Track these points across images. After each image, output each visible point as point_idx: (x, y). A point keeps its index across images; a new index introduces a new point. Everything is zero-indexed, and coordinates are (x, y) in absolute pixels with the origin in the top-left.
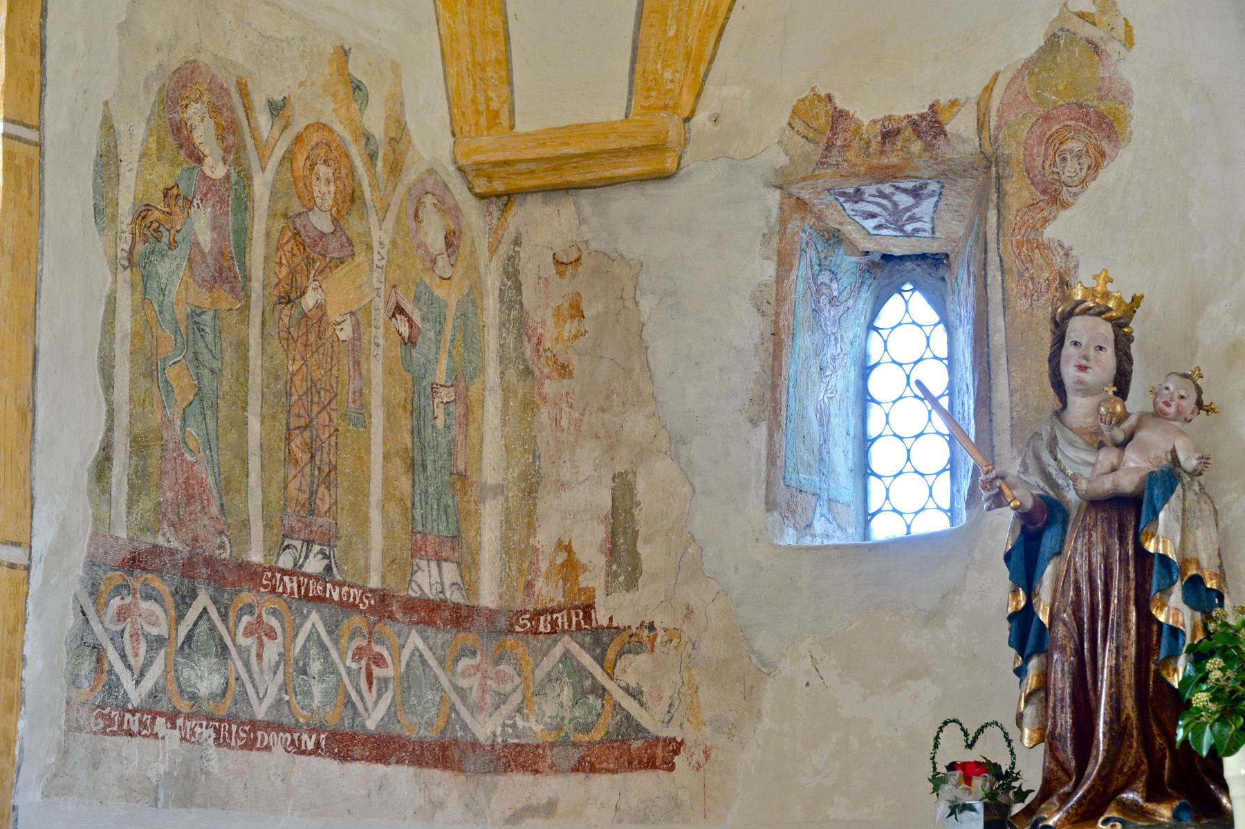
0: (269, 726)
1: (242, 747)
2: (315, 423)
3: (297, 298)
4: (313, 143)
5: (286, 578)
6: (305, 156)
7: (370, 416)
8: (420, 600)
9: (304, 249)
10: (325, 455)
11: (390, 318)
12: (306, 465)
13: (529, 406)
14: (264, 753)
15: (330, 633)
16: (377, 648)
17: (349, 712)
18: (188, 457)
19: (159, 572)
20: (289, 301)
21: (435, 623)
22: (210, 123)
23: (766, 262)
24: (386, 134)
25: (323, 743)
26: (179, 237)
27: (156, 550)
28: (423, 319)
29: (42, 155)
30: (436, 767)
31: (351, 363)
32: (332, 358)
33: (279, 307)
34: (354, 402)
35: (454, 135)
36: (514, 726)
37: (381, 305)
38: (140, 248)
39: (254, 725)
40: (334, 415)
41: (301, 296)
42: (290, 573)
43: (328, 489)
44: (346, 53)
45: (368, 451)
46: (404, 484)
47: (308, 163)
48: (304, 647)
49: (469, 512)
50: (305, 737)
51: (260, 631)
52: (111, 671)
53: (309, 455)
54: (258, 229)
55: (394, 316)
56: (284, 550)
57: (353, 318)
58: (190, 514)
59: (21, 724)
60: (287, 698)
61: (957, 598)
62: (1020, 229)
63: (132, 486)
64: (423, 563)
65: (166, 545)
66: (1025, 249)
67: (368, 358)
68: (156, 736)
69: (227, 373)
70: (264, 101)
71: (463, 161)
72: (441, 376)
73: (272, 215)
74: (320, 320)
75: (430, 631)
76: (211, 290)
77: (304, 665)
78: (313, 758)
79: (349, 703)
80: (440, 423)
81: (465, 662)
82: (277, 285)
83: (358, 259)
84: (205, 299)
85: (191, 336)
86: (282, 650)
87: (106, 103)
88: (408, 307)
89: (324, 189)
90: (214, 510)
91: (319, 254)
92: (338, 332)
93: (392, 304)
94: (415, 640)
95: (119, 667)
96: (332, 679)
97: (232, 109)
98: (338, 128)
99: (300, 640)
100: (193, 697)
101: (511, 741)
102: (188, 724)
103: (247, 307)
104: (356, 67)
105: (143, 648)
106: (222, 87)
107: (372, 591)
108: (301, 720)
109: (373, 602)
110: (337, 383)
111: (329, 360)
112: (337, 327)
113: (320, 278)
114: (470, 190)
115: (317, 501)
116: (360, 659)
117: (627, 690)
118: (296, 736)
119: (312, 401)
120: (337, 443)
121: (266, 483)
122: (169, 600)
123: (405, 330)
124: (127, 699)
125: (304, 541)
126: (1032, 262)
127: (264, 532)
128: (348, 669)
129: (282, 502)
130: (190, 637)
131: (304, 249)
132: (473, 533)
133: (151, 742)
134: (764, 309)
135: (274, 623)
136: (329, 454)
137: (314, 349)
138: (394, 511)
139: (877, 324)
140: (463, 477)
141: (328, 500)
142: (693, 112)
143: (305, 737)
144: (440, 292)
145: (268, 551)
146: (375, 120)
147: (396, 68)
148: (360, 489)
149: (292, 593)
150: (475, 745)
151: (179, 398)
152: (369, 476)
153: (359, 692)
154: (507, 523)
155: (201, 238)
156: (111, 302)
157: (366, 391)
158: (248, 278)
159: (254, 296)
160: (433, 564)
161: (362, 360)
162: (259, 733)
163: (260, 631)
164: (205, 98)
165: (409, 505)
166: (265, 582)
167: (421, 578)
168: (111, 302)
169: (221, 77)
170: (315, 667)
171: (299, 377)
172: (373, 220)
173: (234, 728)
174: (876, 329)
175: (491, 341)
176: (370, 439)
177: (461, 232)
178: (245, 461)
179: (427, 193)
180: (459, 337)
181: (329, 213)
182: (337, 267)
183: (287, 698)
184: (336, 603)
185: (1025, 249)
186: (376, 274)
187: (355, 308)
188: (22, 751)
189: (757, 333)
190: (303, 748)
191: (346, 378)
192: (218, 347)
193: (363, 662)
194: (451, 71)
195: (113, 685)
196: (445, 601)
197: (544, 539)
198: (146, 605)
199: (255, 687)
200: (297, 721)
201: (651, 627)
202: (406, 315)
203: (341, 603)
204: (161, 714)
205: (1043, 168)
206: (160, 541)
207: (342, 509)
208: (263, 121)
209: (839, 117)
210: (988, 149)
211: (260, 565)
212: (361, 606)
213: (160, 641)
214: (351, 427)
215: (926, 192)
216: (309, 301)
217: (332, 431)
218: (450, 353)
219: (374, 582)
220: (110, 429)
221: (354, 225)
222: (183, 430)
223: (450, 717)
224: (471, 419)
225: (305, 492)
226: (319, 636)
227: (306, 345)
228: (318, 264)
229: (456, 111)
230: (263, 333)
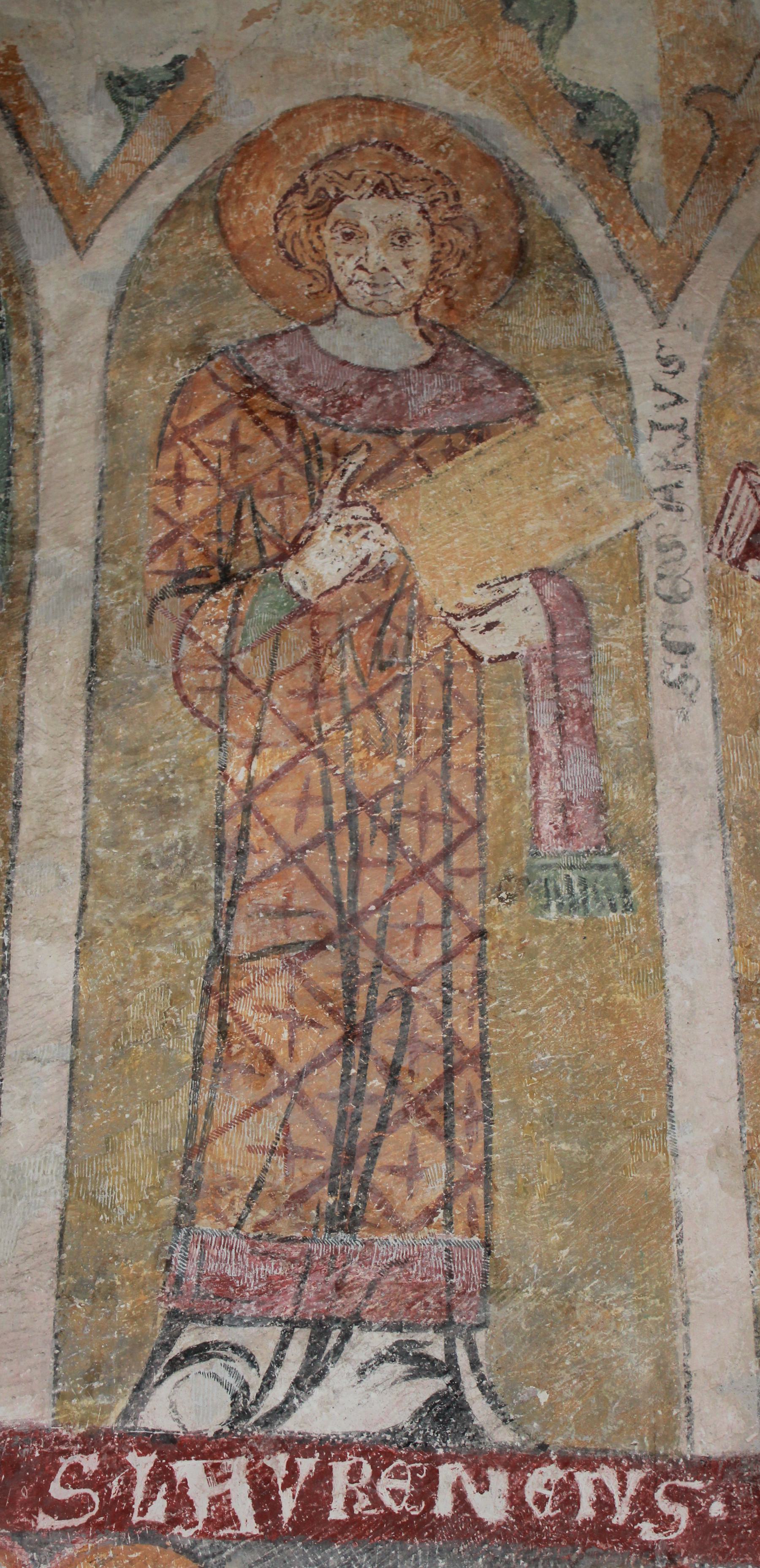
2: (370, 925)
3: (264, 564)
4: (321, 151)
6: (283, 184)
7: (654, 868)
9: (292, 425)
10: (423, 1018)
11: (739, 563)
12: (316, 1064)
20: (227, 578)
24: (666, 79)
31: (544, 721)
32: (447, 717)
33: (176, 605)
34: (568, 834)
41: (283, 557)
47: (299, 203)
53: (337, 1031)
56: (174, 1365)
57: (549, 590)
70: (89, 80)
74: (385, 612)
82: (168, 542)
83: (551, 420)
89: (376, 256)
91: (365, 428)
92: (467, 636)
109: (717, 1509)
110: (480, 787)
111: (432, 723)
112: (467, 623)
113: (372, 495)
115: (379, 1178)
119: (356, 861)
120: (481, 978)
125: (290, 1326)
127: (61, 1316)
129: (171, 1202)
131: (292, 425)
136: (441, 1018)
137: (353, 700)
152: (669, 1065)
161: (603, 701)
166: (57, 1491)
171: (290, 789)
176: (660, 942)
181: (407, 318)
182: (451, 453)
184: (500, 1532)
187: (554, 558)
191: (523, 766)
207: (524, 1190)
211: (35, 1434)
212: (647, 1531)
214: (553, 914)
217: (456, 938)
225: (309, 1153)
227: (313, 696)
228: (359, 458)
230: (90, 687)
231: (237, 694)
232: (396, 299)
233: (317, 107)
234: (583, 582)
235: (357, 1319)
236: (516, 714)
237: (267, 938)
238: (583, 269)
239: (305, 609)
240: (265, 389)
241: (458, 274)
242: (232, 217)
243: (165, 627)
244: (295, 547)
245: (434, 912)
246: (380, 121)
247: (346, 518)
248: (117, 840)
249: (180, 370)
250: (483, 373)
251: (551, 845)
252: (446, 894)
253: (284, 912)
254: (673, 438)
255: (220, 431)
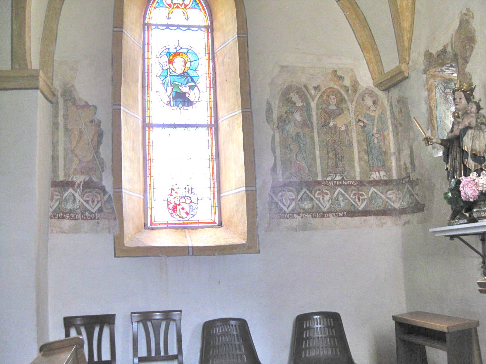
0: (328, 213)
1: (320, 218)
4: (328, 92)
5: (330, 182)
8: (373, 180)
13: (397, 134)
14: (328, 218)
15: (345, 191)
16: (361, 193)
17: (353, 207)
18: (298, 162)
19: (292, 186)
20: (325, 126)
21: (379, 185)
22: (297, 96)
24: (351, 84)
25: (345, 214)
26: (291, 120)
27: (290, 182)
28: (367, 121)
29: (252, 113)
30: (383, 215)
31: (346, 135)
34: (347, 142)
35: (373, 79)
36: (402, 204)
37: (354, 121)
38: (280, 124)
39: (324, 213)
40: (342, 146)
42: (331, 181)
43: (341, 162)
44: (336, 71)
45: (353, 152)
46: (366, 157)
48: (337, 194)
49: (388, 159)
50: (339, 214)
51: (323, 194)
52: (280, 207)
54: (314, 113)
55: (358, 122)
58: (300, 173)
59: (258, 219)
60: (333, 206)
63: (283, 171)
64: (374, 173)
65: (293, 180)
67: (351, 133)
68: (294, 218)
69: (308, 144)
70: (312, 87)
71: (375, 85)
72: (375, 131)
73: (317, 109)
74: (335, 128)
75: (378, 187)
76: (301, 129)
77: (338, 199)
78: (343, 218)
79: (352, 205)
80: (376, 142)
81: (389, 193)
83: (345, 113)
84: (300, 130)
85: (297, 138)
86: (330, 197)
87: (267, 99)
88: (362, 119)
90: (307, 171)
93: (357, 120)
94: (373, 189)
95: (282, 206)
96: (347, 201)
97: (302, 91)
98: (335, 87)
99: (336, 194)
100: (304, 209)
101: (402, 208)
102: (303, 215)
103: (313, 129)
104: (340, 73)
105: (289, 202)
106: (300, 88)
107: (357, 181)
108: (338, 210)
114: (380, 90)
116: (355, 195)
117: (415, 194)
118: (337, 214)
120: (343, 152)
121: (322, 163)
122: (295, 192)
123: (362, 124)
124: (285, 212)
128: (352, 198)
130: (301, 197)
132: (389, 164)
133: (293, 219)
135: (327, 191)
136: (341, 155)
138: (362, 163)
140: (385, 153)
141: (341, 164)
142: (409, 61)
143: (339, 214)
144: (373, 114)
145: (323, 177)
146: (347, 82)
147: (352, 70)
148: (352, 159)
149: (332, 185)
150: (395, 209)
151: (294, 151)
153: (355, 202)
154: (396, 160)
155: (297, 119)
156: (273, 137)
157: (351, 140)
158: (312, 124)
159: (314, 127)
160: (377, 173)
162: (325, 214)
163: (323, 194)
164: (295, 91)
165: (368, 161)
166: (323, 184)
167: (372, 176)
168: (273, 137)
169: (299, 86)
170: (341, 199)
171: (330, 140)
172: (349, 104)
173: (317, 214)
175: (389, 121)
177: (378, 100)
178: (315, 160)
179: (366, 94)
180: (379, 122)
182: (339, 116)
183: (333, 206)
186: (351, 115)
187: (345, 123)
188: (258, 224)
190: (339, 215)
191: (344, 138)
192: (305, 140)
193: (357, 196)
194: (370, 66)
195: (281, 209)
196: (382, 180)
197: (402, 163)
198: (288, 193)
199: (322, 205)
200: (337, 211)
201: (418, 179)
202: (362, 121)
203: (348, 185)
204: (295, 214)
206: (292, 180)
208: (313, 92)
209: (431, 54)
210: (454, 53)
213: (293, 199)
216: (331, 124)
218: (377, 126)
219: (358, 179)
220: (275, 161)
221: (343, 106)
222: (296, 158)
223: (386, 204)
224: (385, 139)
226: (341, 192)
229: (373, 74)
230: (318, 134)
231: (327, 134)
232: (334, 104)
233: (328, 89)
234: (347, 125)
235: (337, 173)
236: (344, 134)
237: (331, 150)
238: (346, 101)
239: (330, 128)
240: (326, 111)
241: (338, 102)
242: (323, 98)
243: (322, 129)
244: (329, 123)
245: (340, 148)
246: (332, 89)
247: (332, 121)
248: (321, 144)
249: (321, 110)
250: (340, 110)
251: (347, 143)
252: (340, 147)
253: (331, 148)
254: (352, 114)
255: (324, 115)
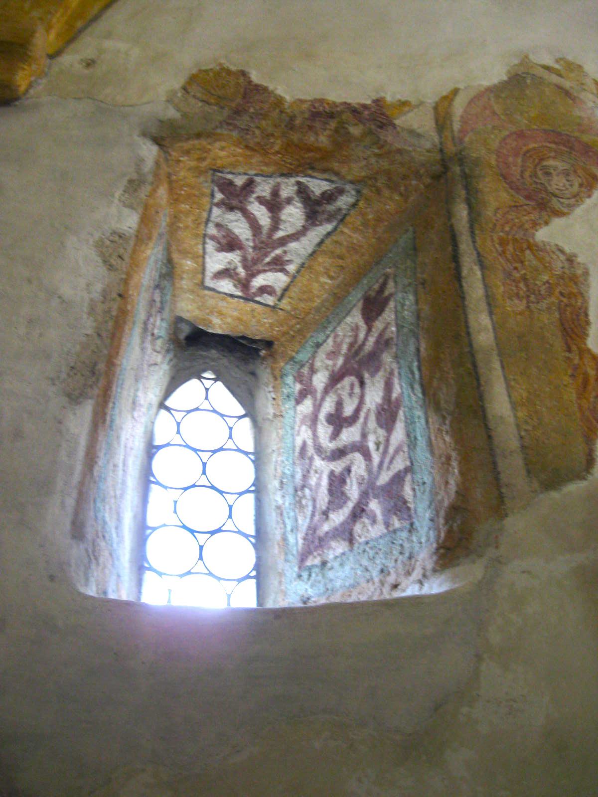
23: (126, 211)
61: (465, 710)
62: (503, 225)
66: (510, 248)
126: (522, 262)
134: (114, 263)
139: (168, 403)
174: (168, 409)
185: (510, 248)
189: (98, 287)
205: (522, 177)
210: (451, 149)
215: (331, 208)
